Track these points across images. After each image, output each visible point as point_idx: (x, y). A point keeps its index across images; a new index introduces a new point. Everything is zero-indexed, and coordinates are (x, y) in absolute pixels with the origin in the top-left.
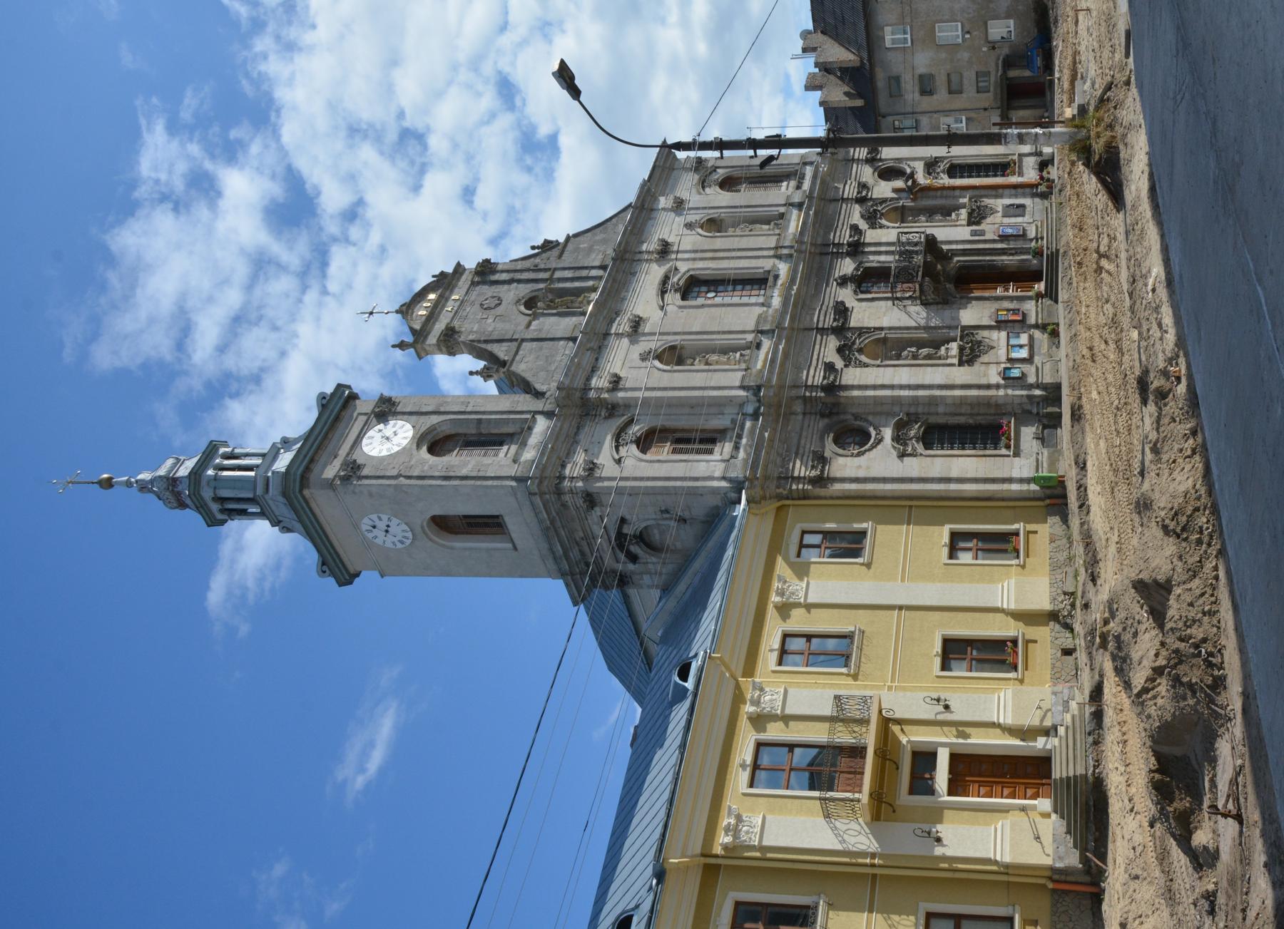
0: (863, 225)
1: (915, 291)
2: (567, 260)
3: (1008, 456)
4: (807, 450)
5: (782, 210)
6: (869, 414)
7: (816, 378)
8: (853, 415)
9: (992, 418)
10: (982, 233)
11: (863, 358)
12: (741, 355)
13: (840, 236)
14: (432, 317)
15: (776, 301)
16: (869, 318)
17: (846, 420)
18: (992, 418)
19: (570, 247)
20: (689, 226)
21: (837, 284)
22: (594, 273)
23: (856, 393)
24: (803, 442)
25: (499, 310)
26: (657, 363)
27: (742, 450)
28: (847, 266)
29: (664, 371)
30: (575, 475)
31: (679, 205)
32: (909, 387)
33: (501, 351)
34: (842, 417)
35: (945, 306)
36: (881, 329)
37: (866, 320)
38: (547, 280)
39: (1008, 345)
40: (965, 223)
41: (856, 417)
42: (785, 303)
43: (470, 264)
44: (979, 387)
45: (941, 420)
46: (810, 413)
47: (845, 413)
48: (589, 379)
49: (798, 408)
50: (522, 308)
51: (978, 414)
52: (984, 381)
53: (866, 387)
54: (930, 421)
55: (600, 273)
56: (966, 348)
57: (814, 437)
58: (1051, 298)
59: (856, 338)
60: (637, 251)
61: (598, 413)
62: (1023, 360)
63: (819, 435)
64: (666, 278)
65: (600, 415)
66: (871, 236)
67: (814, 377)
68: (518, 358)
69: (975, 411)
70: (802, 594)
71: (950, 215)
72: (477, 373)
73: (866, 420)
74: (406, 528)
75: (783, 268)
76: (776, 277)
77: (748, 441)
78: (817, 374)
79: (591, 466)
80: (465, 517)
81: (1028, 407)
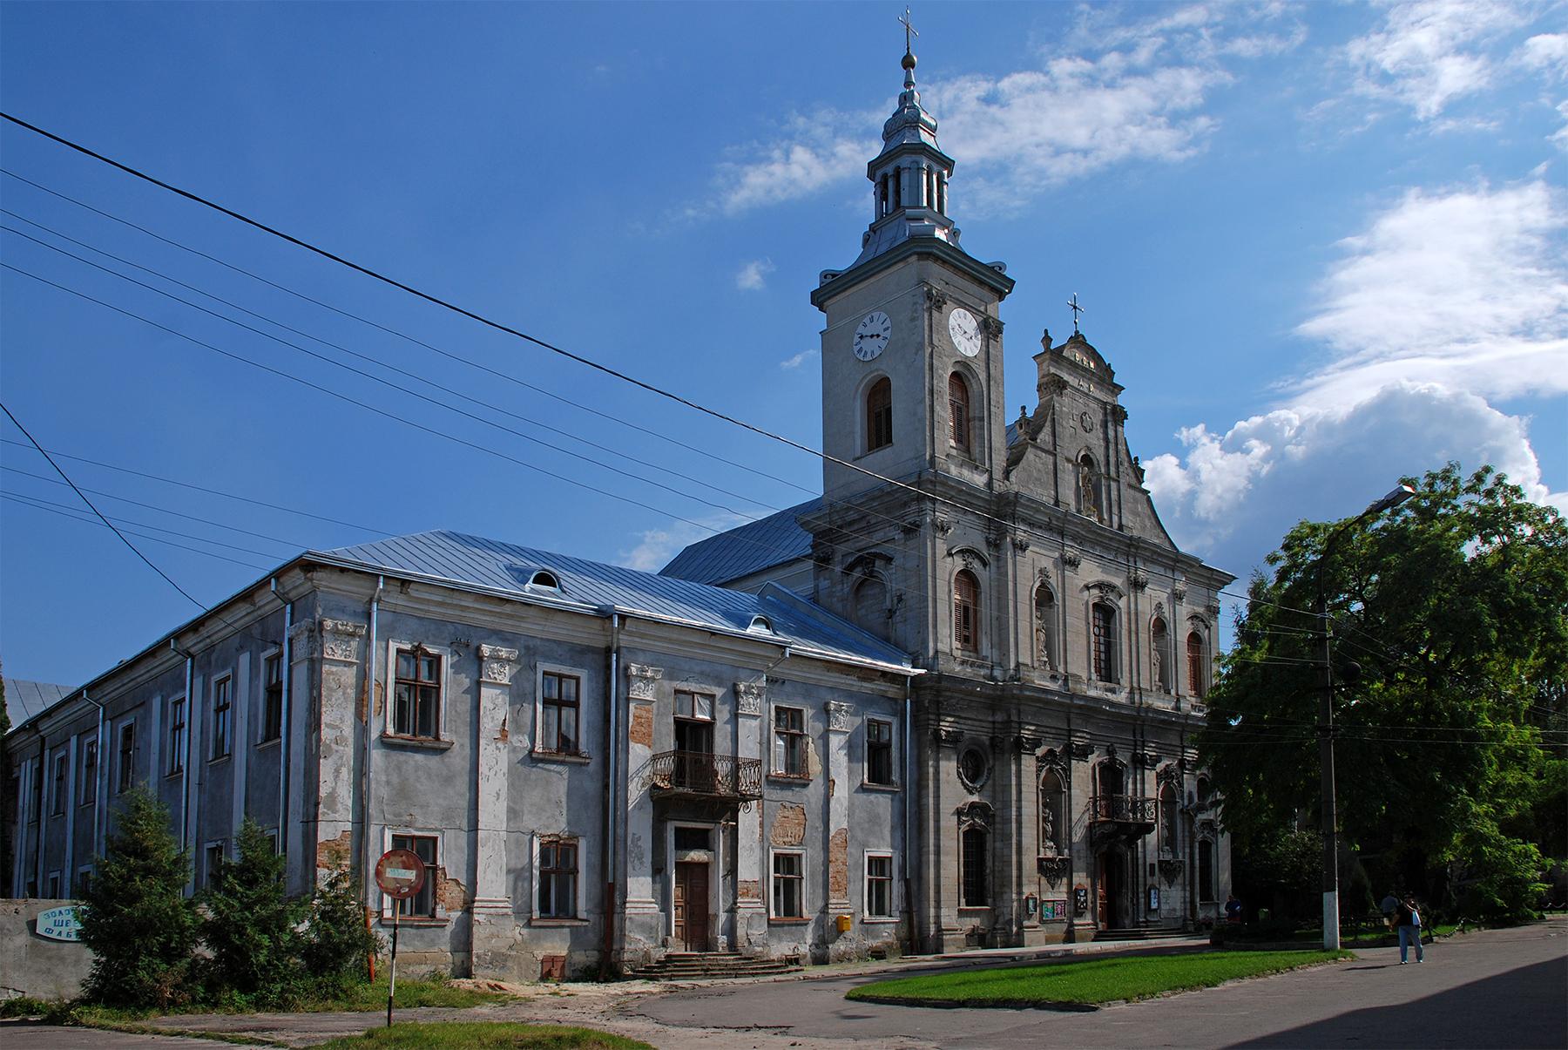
0: (1160, 766)
2: (1127, 493)
4: (963, 727)
5: (1173, 692)
6: (994, 780)
8: (993, 766)
10: (1152, 874)
11: (1043, 774)
12: (1045, 662)
14: (1074, 366)
15: (1092, 693)
16: (1079, 776)
17: (988, 761)
19: (1139, 495)
20: (1159, 606)
21: (1108, 746)
22: (1115, 519)
23: (1014, 767)
24: (970, 722)
25: (1080, 431)
26: (1037, 584)
28: (1123, 757)
29: (1031, 591)
30: (937, 513)
31: (1177, 597)
32: (1019, 815)
33: (1044, 436)
34: (990, 757)
35: (1088, 845)
36: (1069, 789)
37: (1077, 774)
38: (1109, 474)
40: (1161, 858)
41: (991, 770)
42: (1093, 699)
43: (1121, 400)
44: (1019, 877)
45: (989, 846)
46: (994, 728)
47: (994, 759)
48: (1024, 521)
49: (999, 717)
50: (1083, 453)
51: (994, 878)
52: (1025, 880)
53: (1019, 777)
54: (988, 835)
55: (1116, 526)
57: (973, 733)
58: (1096, 936)
59: (1061, 765)
60: (1137, 559)
61: (992, 531)
64: (1112, 587)
65: (990, 533)
66: (1151, 776)
68: (1039, 452)
69: (997, 874)
70: (837, 727)
71: (1167, 845)
74: (877, 354)
75: (1122, 697)
76: (1113, 691)
79: (945, 528)
80: (889, 411)
81: (1001, 920)
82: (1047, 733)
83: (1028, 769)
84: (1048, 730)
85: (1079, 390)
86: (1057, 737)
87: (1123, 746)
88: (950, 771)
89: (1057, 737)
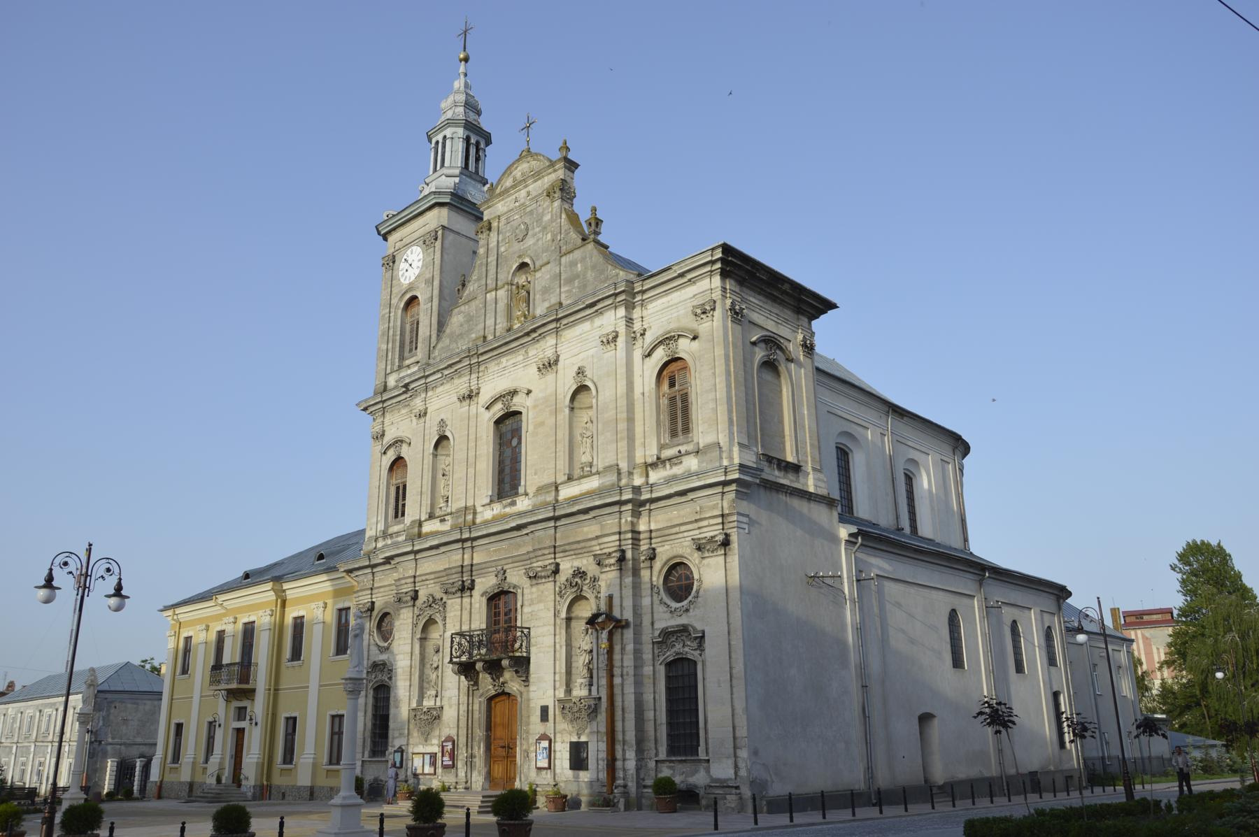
1: (456, 658)
7: (406, 586)
13: (544, 555)
15: (486, 514)
24: (382, 590)
37: (452, 614)
39: (423, 754)
57: (386, 597)
63: (389, 600)
67: (406, 583)
68: (462, 308)
78: (409, 585)
82: (427, 580)
83: (405, 622)
84: (427, 577)
85: (516, 207)
86: (436, 580)
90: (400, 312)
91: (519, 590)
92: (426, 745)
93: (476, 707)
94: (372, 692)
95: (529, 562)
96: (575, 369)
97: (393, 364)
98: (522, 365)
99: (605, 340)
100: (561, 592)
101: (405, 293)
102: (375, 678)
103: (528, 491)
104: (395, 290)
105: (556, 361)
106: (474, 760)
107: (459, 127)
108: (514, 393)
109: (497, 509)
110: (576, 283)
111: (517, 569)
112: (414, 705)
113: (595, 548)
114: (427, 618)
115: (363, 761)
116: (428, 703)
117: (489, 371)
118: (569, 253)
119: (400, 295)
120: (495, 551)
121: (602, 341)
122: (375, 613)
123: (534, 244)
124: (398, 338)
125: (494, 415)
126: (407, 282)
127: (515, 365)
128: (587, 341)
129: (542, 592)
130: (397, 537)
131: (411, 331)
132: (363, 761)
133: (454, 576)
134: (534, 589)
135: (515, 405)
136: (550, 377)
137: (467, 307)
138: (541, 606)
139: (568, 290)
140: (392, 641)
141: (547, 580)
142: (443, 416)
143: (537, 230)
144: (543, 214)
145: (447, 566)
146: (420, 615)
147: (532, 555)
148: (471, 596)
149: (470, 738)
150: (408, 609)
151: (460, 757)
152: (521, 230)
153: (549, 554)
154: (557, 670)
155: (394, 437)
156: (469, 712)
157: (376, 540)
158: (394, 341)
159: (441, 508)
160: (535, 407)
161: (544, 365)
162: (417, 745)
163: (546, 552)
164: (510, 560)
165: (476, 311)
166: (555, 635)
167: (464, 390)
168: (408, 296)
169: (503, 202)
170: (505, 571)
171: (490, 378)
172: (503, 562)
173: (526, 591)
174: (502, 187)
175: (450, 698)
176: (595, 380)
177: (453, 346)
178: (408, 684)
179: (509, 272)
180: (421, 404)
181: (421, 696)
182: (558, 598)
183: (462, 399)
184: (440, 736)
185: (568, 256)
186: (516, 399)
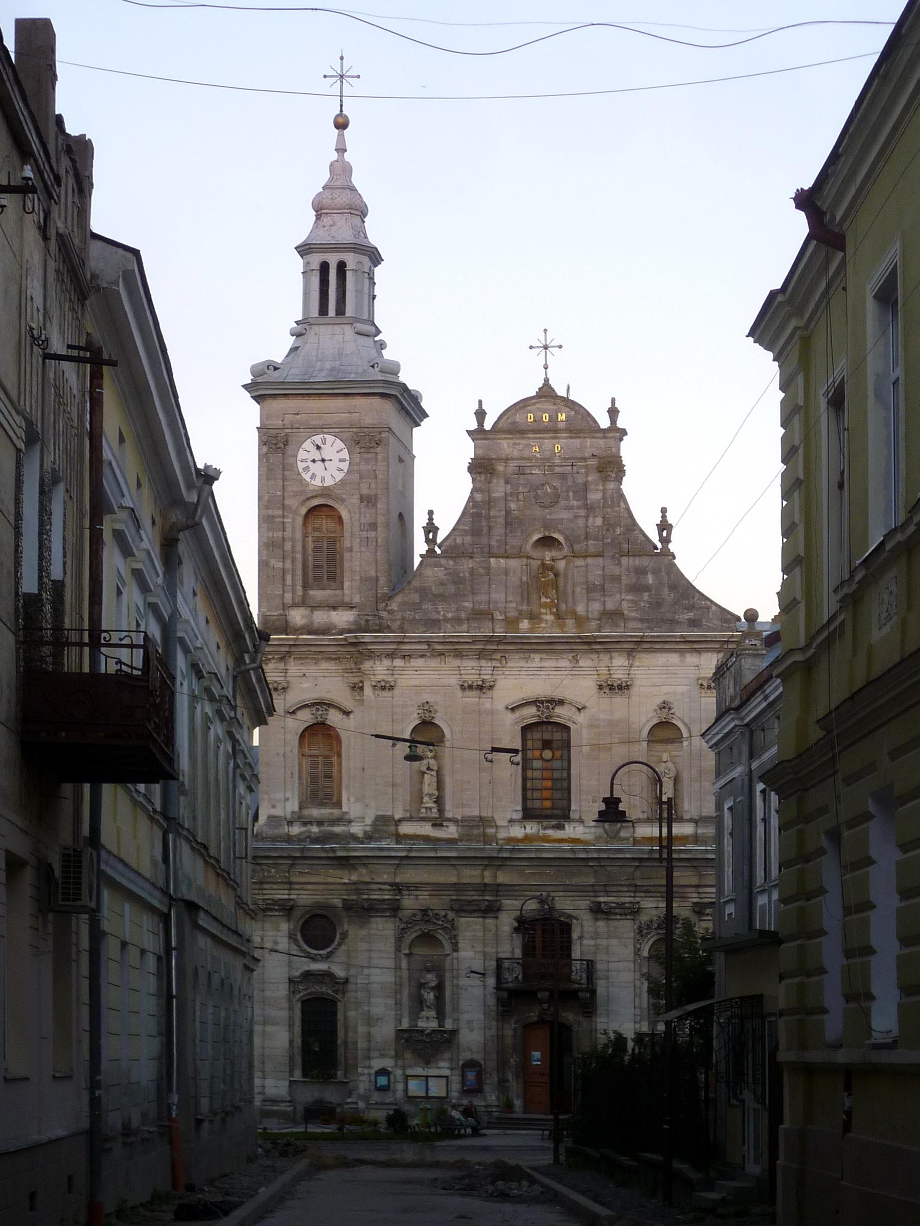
3: (292, 1075)
7: (379, 893)
9: (343, 1059)
15: (517, 832)
18: (343, 1061)
24: (309, 887)
27: (303, 829)
36: (456, 950)
37: (468, 934)
39: (427, 1077)
41: (344, 936)
54: (339, 1004)
56: (422, 1036)
57: (318, 897)
62: (406, 1090)
68: (443, 561)
72: (431, 519)
73: (340, 944)
77: (315, 833)
85: (537, 459)
86: (433, 893)
87: (569, 894)
88: (279, 939)
89: (433, 893)
90: (299, 521)
91: (574, 921)
92: (428, 1068)
93: (509, 1032)
94: (298, 1007)
95: (591, 894)
96: (658, 701)
97: (294, 592)
98: (567, 673)
99: (705, 684)
100: (641, 931)
101: (313, 497)
102: (306, 989)
103: (583, 818)
104: (292, 488)
105: (628, 687)
106: (506, 1084)
107: (364, 254)
108: (561, 702)
109: (532, 828)
110: (646, 596)
111: (572, 898)
112: (405, 1025)
113: (689, 895)
114: (419, 933)
115: (291, 1081)
116: (428, 1023)
117: (509, 665)
118: (634, 556)
119: (303, 498)
120: (535, 874)
121: (702, 685)
122: (298, 913)
123: (570, 521)
124: (299, 556)
125: (523, 719)
126: (317, 482)
127: (558, 669)
128: (675, 676)
129: (616, 928)
130: (332, 825)
131: (317, 549)
132: (291, 1081)
133: (470, 893)
134: (601, 923)
135: (559, 717)
136: (619, 700)
137: (451, 562)
138: (614, 942)
139: (632, 600)
140: (334, 949)
141: (624, 917)
142: (426, 697)
143: (575, 503)
144: (585, 487)
145: (454, 879)
146: (408, 928)
147: (597, 888)
148: (496, 918)
149: (502, 1064)
150: (384, 919)
151: (488, 1081)
152: (546, 494)
153: (627, 892)
154: (637, 1005)
155: (316, 696)
156: (500, 1038)
157: (290, 823)
158: (294, 560)
159: (430, 809)
160: (591, 726)
161: (612, 685)
162: (411, 1066)
163: (625, 889)
164: (561, 888)
165: (472, 571)
166: (635, 971)
167: (472, 678)
168: (316, 502)
169: (511, 442)
170: (553, 899)
171: (514, 673)
172: (550, 889)
173: (585, 923)
174: (508, 418)
175: (470, 1022)
176: (687, 720)
177: (427, 606)
178: (392, 1002)
179: (527, 541)
180: (385, 672)
181: (415, 1017)
182: (638, 937)
183: (466, 687)
184: (451, 1060)
185: (632, 558)
186: (559, 710)
